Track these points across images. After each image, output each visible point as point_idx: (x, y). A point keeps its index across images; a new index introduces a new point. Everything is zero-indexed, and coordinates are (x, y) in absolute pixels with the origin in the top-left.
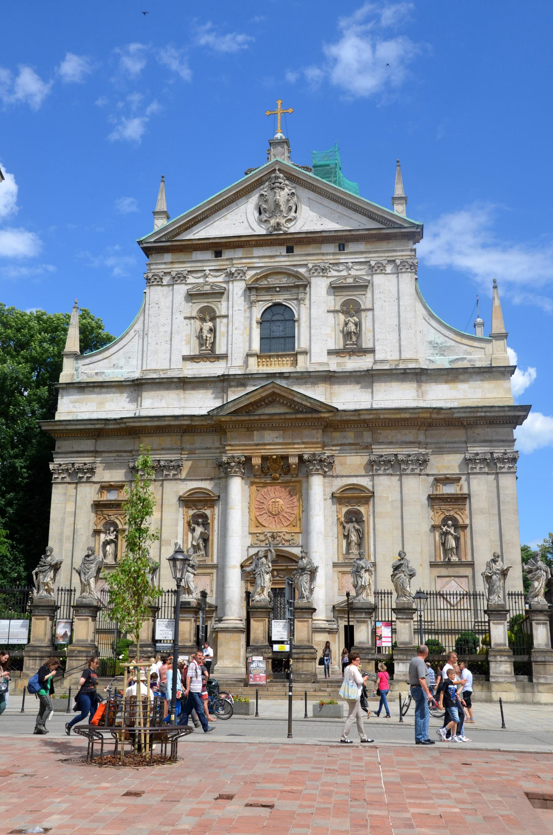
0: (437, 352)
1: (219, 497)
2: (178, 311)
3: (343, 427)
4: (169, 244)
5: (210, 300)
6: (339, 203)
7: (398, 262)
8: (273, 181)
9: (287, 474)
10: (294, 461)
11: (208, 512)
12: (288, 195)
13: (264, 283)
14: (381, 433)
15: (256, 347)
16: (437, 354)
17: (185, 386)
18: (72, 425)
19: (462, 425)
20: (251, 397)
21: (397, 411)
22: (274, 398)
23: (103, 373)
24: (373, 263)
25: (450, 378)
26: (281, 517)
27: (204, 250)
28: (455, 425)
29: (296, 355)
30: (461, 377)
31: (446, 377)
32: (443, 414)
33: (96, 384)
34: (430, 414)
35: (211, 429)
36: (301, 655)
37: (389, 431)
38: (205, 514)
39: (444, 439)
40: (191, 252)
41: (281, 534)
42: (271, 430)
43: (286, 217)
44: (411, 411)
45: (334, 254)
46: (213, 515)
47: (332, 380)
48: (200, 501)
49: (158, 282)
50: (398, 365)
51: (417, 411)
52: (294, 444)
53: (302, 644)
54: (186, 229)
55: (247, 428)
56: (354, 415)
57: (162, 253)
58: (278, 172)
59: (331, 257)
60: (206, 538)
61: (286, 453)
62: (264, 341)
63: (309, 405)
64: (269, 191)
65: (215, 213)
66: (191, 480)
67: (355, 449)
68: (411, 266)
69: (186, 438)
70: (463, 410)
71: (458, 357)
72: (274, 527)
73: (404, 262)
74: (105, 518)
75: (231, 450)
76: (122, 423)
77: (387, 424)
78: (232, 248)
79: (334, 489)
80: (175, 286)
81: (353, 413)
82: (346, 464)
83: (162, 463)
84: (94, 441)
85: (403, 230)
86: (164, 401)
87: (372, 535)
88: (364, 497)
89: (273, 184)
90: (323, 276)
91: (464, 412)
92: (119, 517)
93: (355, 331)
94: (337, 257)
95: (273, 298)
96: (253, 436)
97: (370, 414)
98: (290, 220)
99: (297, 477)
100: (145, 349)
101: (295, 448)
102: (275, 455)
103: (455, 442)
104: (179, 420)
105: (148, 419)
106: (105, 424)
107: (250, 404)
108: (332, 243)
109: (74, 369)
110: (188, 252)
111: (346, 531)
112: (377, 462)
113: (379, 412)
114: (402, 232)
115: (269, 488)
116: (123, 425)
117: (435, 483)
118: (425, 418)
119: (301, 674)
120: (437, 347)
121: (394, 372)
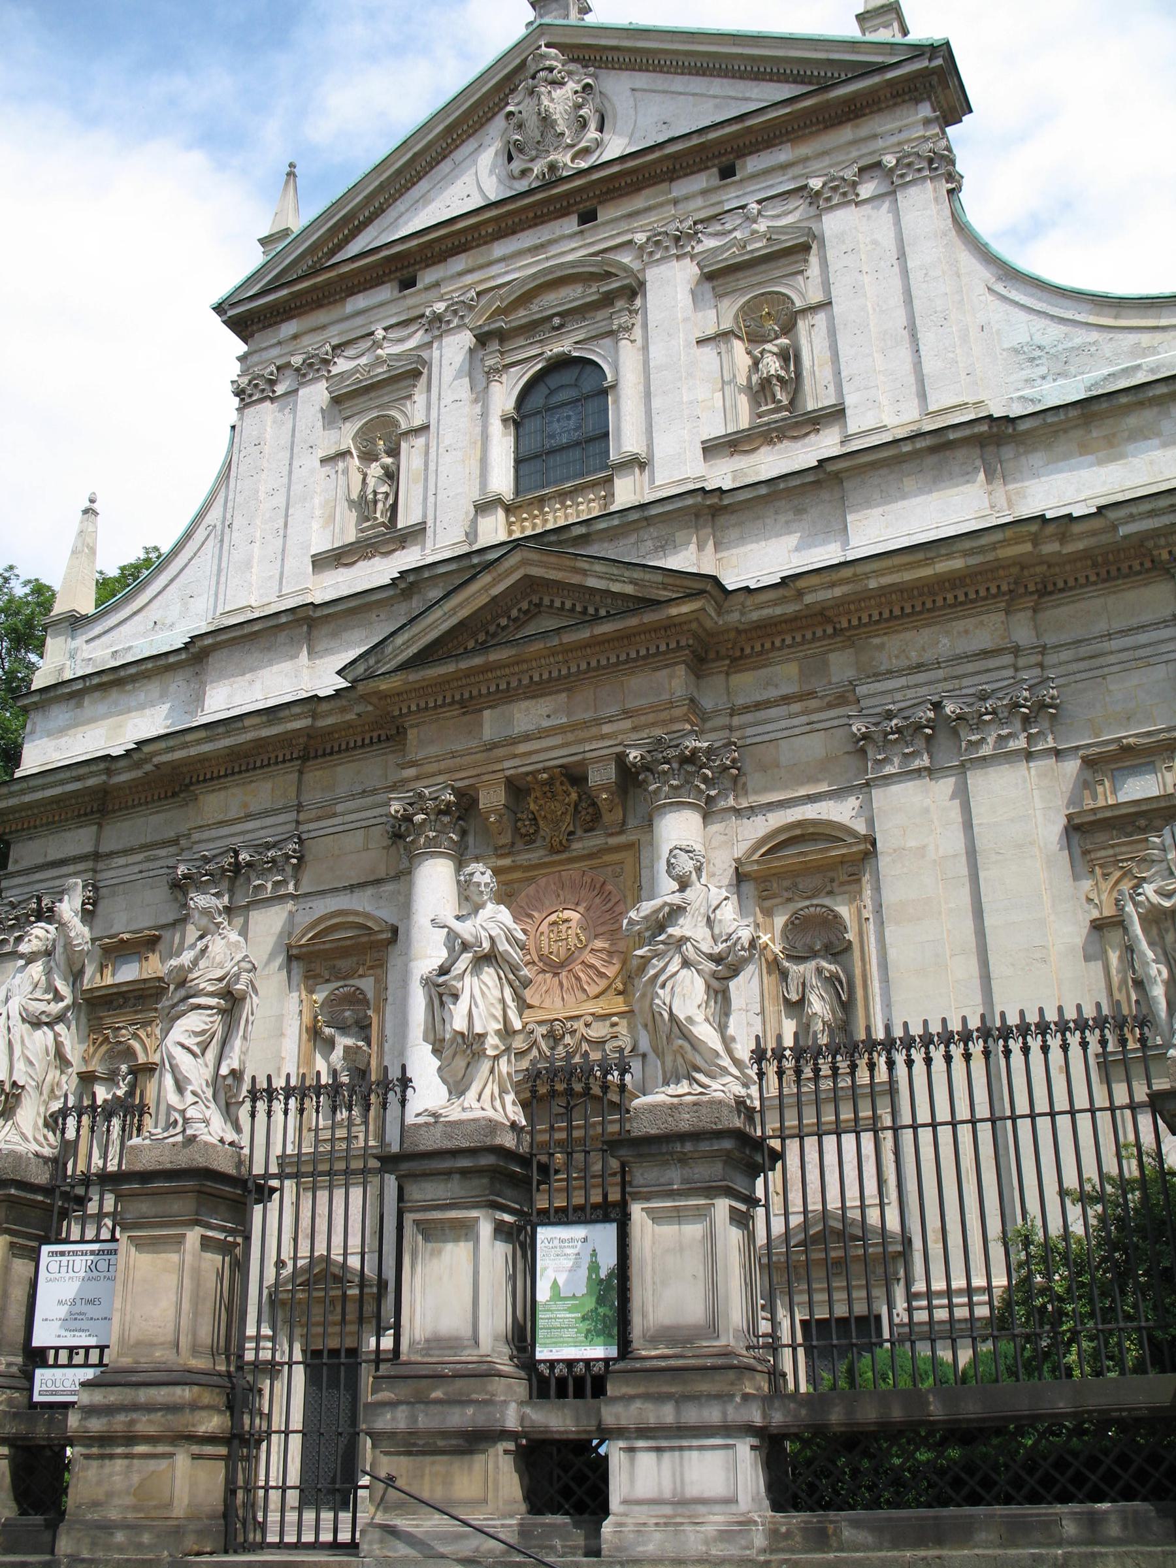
0: (1043, 370)
1: (395, 931)
2: (306, 446)
3: (758, 648)
4: (285, 292)
5: (386, 399)
6: (711, 75)
7: (890, 160)
8: (532, 71)
9: (592, 829)
10: (601, 776)
11: (367, 985)
12: (576, 92)
13: (521, 316)
14: (883, 645)
15: (502, 481)
16: (1044, 378)
17: (315, 633)
18: (33, 790)
19: (1154, 568)
20: (461, 605)
21: (920, 556)
22: (536, 600)
23: (130, 648)
24: (816, 183)
25: (1095, 434)
26: (578, 968)
27: (371, 287)
28: (1131, 572)
29: (609, 480)
30: (1132, 421)
31: (1079, 433)
32: (1081, 536)
33: (105, 679)
34: (1035, 544)
35: (375, 735)
36: (121, 1418)
37: (908, 635)
38: (362, 993)
39: (1102, 626)
40: (343, 300)
41: (579, 1025)
42: (533, 697)
43: (573, 146)
44: (968, 544)
45: (704, 192)
46: (382, 987)
47: (722, 520)
48: (343, 951)
49: (263, 391)
50: (919, 429)
51: (983, 541)
52: (598, 722)
53: (144, 1362)
54: (333, 252)
55: (463, 704)
56: (783, 600)
57: (276, 323)
58: (543, 48)
59: (699, 202)
60: (362, 1067)
61: (580, 757)
62: (525, 468)
63: (629, 589)
64: (528, 100)
65: (402, 195)
66: (322, 893)
67: (805, 712)
68: (931, 161)
69: (315, 775)
70: (1146, 507)
71: (1111, 370)
72: (558, 1003)
73: (909, 155)
74: (107, 1039)
75: (417, 778)
76: (147, 760)
77: (897, 612)
78: (440, 262)
79: (740, 850)
80: (301, 392)
81: (781, 592)
82: (778, 766)
83: (244, 856)
84: (95, 828)
85: (890, 75)
86: (258, 685)
87: (876, 986)
88: (842, 861)
89: (533, 77)
90: (678, 257)
91: (1152, 514)
92: (142, 1034)
93: (783, 373)
94: (714, 198)
95: (546, 349)
96: (481, 725)
97: (833, 585)
98: (586, 151)
99: (621, 832)
100: (224, 565)
101: (603, 737)
102: (545, 770)
103: (1142, 628)
104: (281, 720)
105: (202, 734)
106: (109, 772)
107: (461, 624)
108: (700, 171)
109: (67, 656)
110: (335, 301)
111: (792, 988)
112: (879, 738)
113: (860, 569)
114: (890, 83)
115: (543, 882)
116: (148, 767)
117: (1088, 775)
118: (1022, 564)
119: (107, 1527)
120: (1040, 357)
121: (907, 448)
